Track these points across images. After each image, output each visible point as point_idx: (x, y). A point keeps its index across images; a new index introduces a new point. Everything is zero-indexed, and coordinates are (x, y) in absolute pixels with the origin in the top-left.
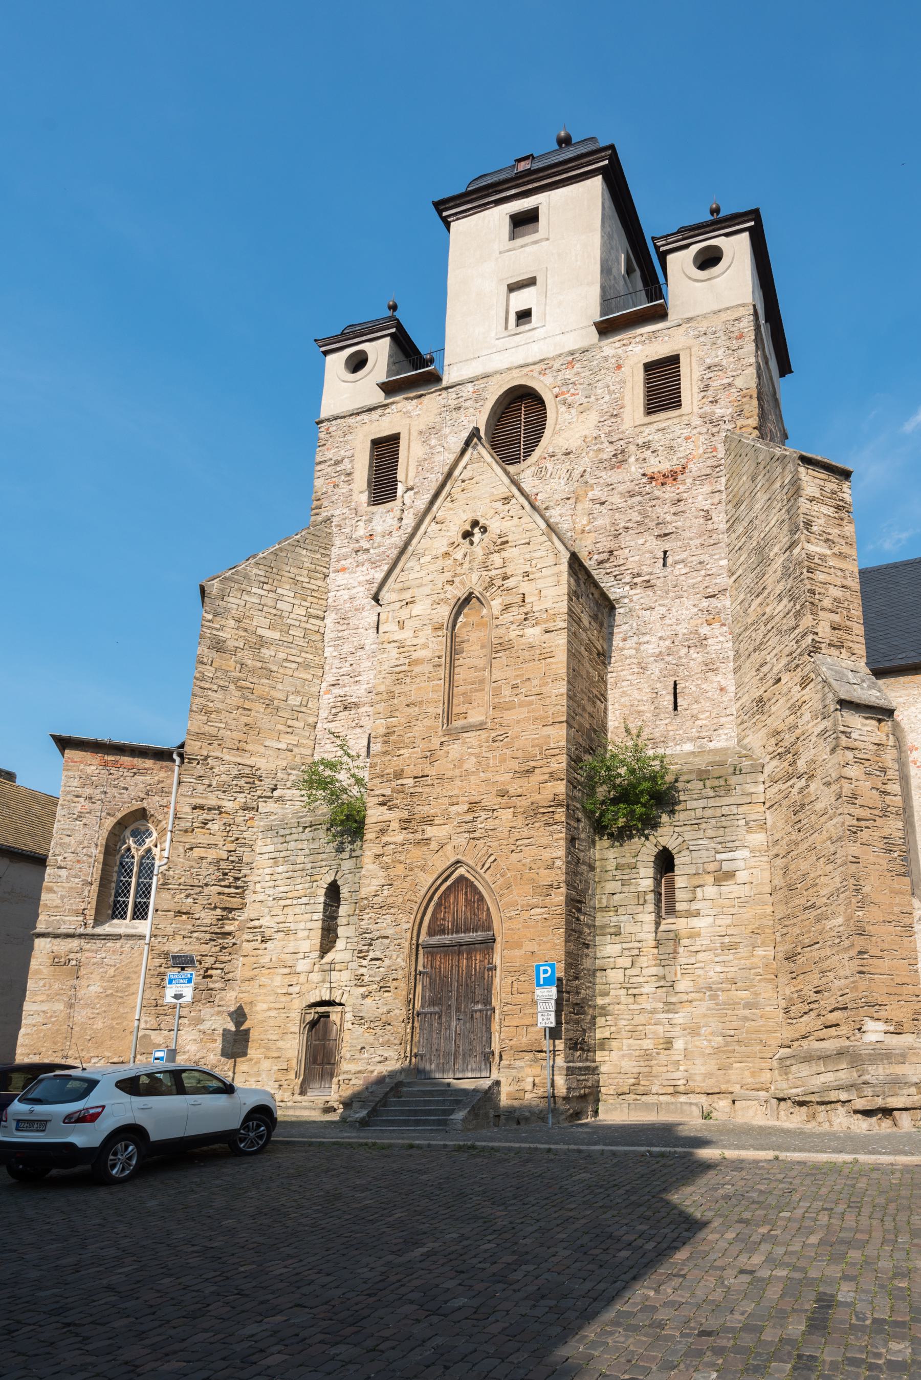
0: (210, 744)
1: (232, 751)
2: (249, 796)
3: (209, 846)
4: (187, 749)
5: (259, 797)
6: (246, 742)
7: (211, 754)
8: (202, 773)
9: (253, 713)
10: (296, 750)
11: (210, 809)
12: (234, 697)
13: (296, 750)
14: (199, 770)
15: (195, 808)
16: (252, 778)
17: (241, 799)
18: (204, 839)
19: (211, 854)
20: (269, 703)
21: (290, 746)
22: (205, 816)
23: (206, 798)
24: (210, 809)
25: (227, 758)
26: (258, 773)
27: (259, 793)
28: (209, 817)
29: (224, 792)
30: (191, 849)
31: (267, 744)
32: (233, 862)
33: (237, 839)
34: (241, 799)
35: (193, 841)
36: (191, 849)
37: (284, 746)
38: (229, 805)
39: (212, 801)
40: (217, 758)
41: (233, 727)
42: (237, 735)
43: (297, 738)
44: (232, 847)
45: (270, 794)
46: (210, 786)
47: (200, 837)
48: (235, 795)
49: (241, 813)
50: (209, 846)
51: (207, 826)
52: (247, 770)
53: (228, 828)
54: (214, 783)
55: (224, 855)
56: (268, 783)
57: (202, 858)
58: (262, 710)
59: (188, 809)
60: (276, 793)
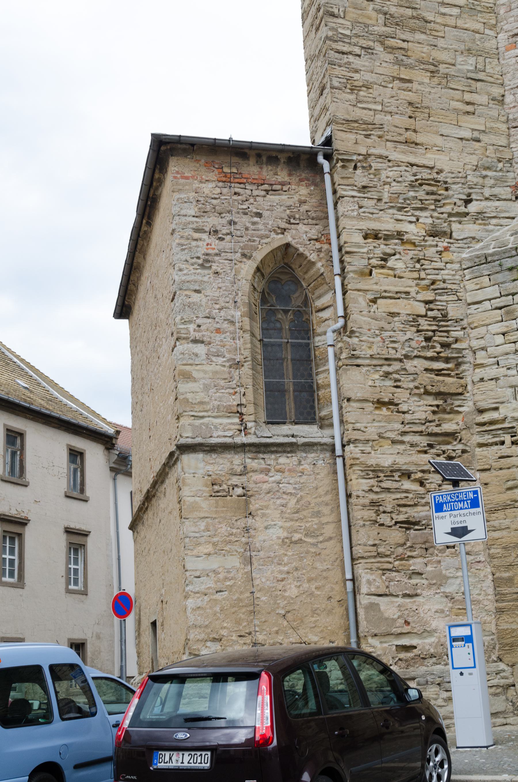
0: (367, 136)
1: (399, 146)
2: (435, 214)
3: (397, 296)
4: (337, 145)
5: (450, 215)
6: (415, 131)
7: (372, 151)
8: (365, 181)
9: (415, 86)
10: (484, 138)
11: (387, 238)
12: (383, 64)
13: (484, 138)
14: (360, 177)
15: (366, 237)
16: (432, 186)
17: (426, 219)
18: (391, 285)
19: (404, 307)
20: (433, 68)
21: (476, 134)
22: (383, 248)
23: (378, 220)
24: (387, 238)
25: (394, 156)
26: (441, 177)
27: (448, 209)
28: (388, 251)
29: (400, 209)
30: (374, 301)
31: (444, 132)
32: (434, 318)
33: (433, 283)
34: (426, 219)
35: (375, 287)
36: (374, 301)
37: (467, 134)
38: (413, 231)
39: (386, 223)
40: (380, 157)
41: (393, 109)
42: (402, 121)
43: (482, 120)
44: (429, 296)
45: (462, 209)
46: (379, 200)
47: (381, 281)
48: (417, 213)
49: (431, 241)
50: (397, 296)
51: (390, 264)
52: (425, 174)
53: (418, 266)
54: (386, 197)
55: (421, 309)
56: (457, 192)
57: (393, 315)
58: (427, 80)
59: (358, 238)
60: (473, 208)
